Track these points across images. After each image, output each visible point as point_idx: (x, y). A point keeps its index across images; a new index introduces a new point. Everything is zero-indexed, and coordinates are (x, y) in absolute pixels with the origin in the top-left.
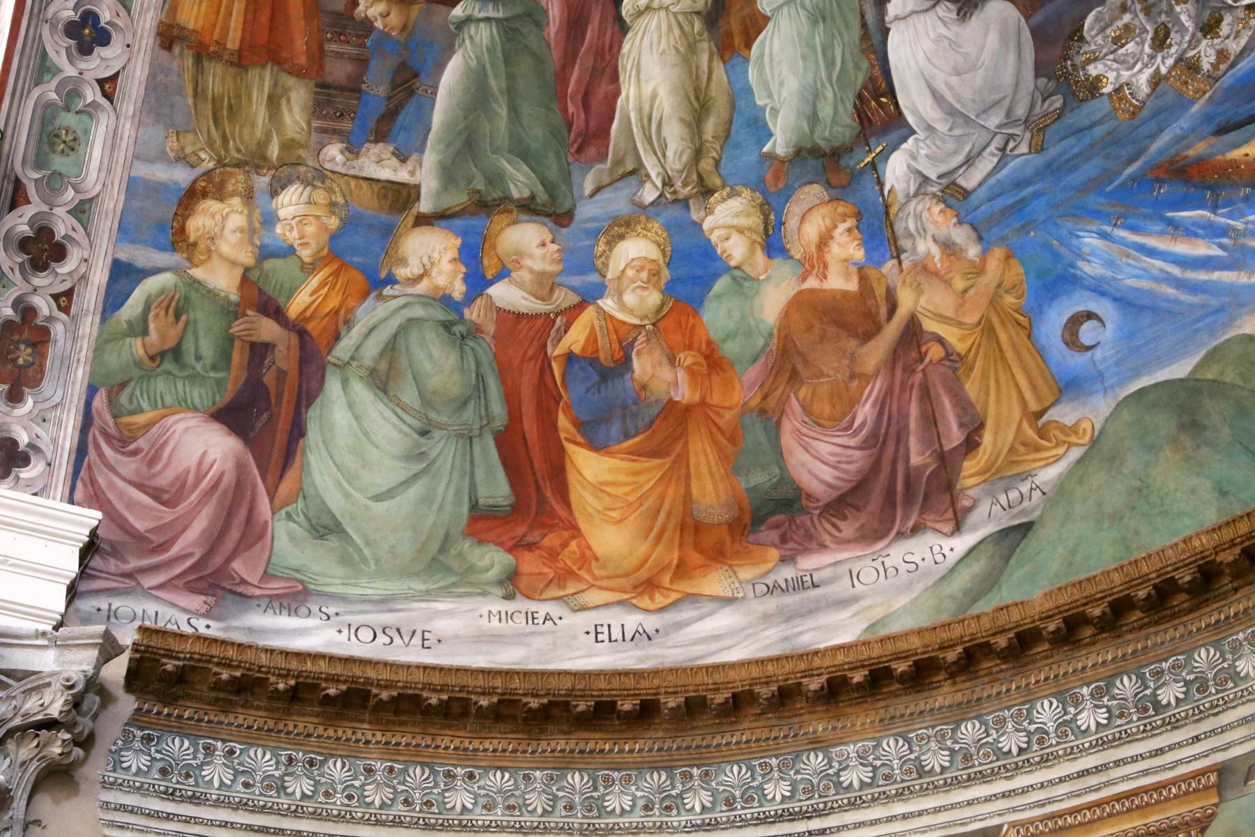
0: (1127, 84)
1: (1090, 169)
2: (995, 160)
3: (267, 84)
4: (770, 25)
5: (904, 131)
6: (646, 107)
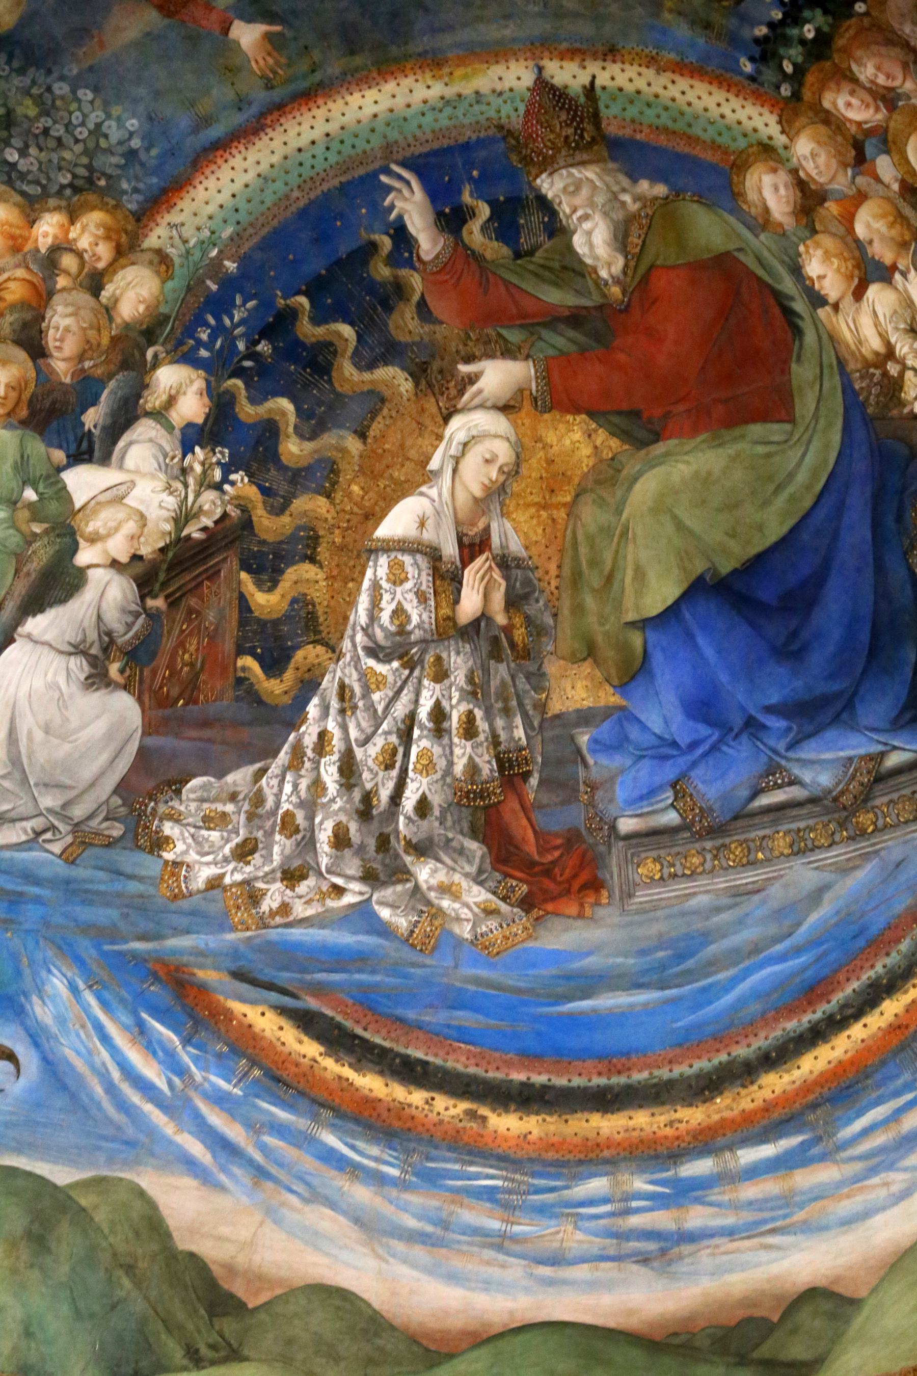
0: (188, 866)
1: (104, 915)
2: (24, 838)
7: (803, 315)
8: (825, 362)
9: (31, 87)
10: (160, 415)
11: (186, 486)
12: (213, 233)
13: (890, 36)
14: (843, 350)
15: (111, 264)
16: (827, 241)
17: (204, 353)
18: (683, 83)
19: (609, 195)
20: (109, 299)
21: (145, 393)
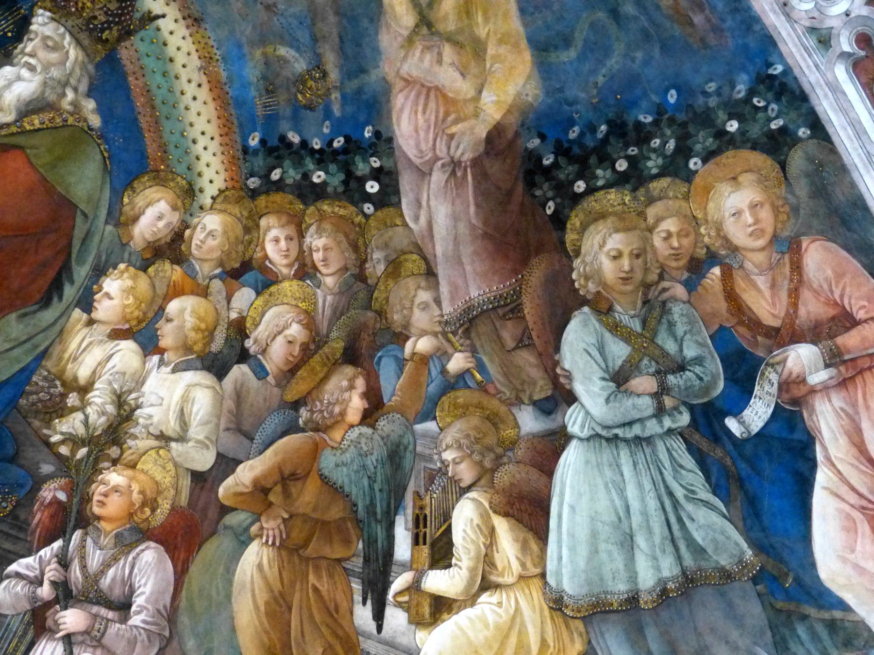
7: (64, 300)
8: (35, 341)
13: (361, 242)
14: (56, 351)
16: (143, 283)
18: (204, 94)
19: (63, 79)
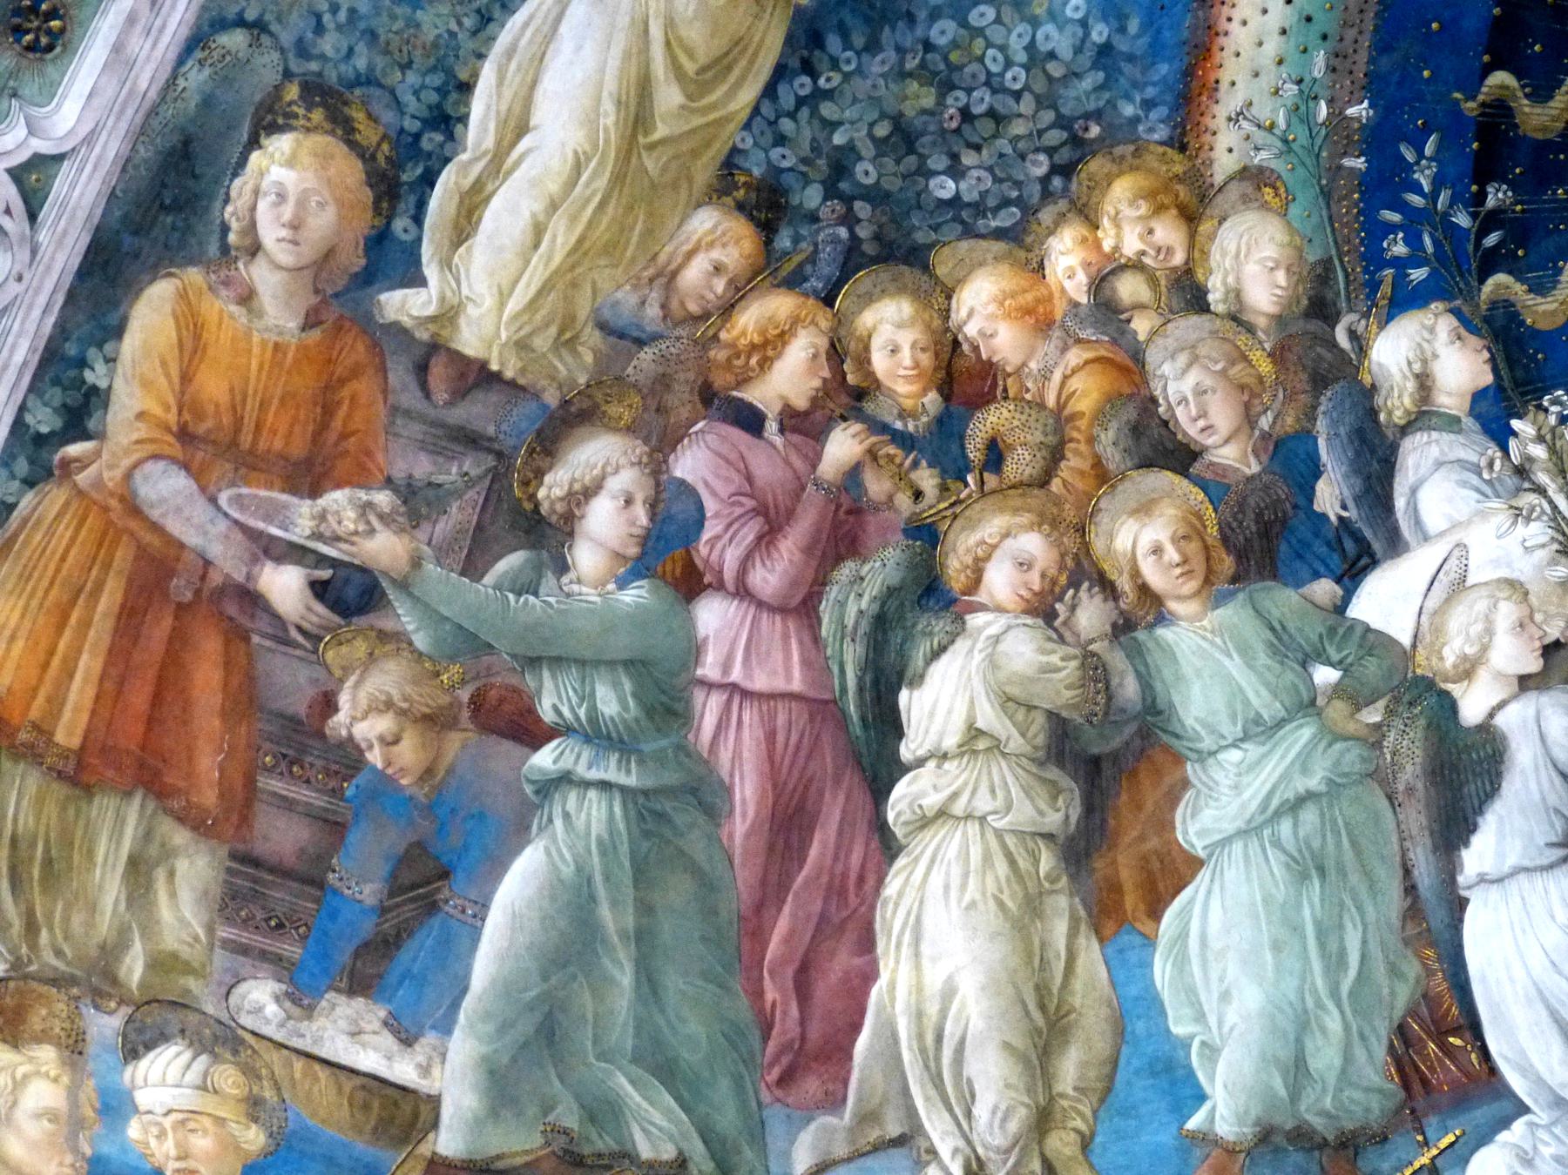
3: (129, 831)
4: (1204, 876)
5: (1505, 1106)
6: (932, 1010)
9: (902, 62)
10: (1424, 417)
11: (1541, 491)
12: (1300, 82)
15: (1191, 246)
17: (1418, 274)
20: (1225, 301)
21: (1379, 400)
